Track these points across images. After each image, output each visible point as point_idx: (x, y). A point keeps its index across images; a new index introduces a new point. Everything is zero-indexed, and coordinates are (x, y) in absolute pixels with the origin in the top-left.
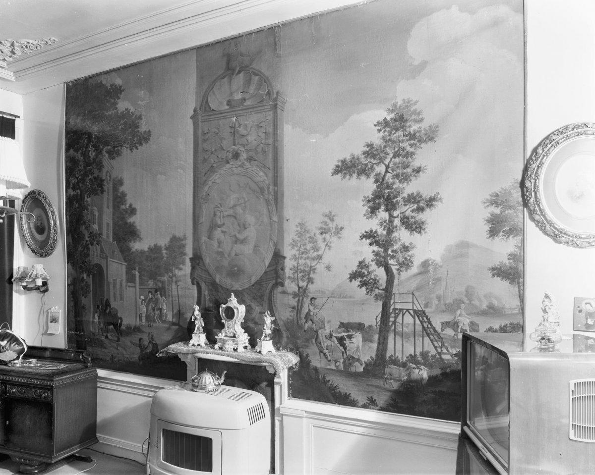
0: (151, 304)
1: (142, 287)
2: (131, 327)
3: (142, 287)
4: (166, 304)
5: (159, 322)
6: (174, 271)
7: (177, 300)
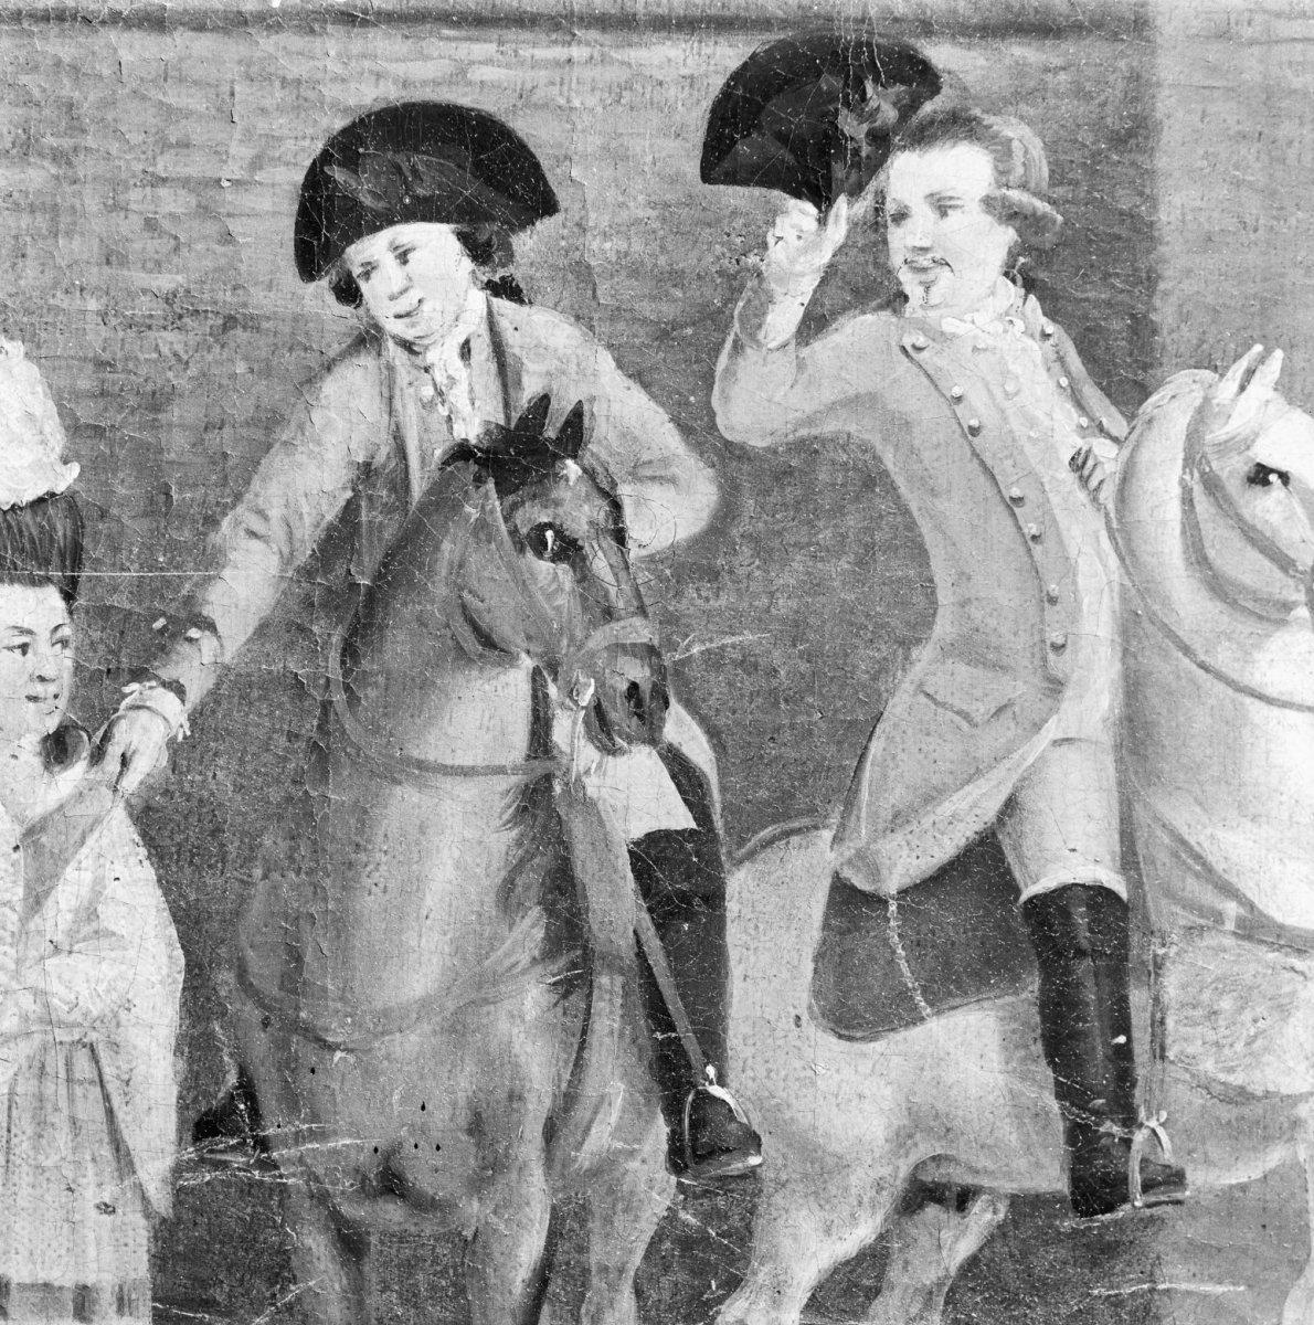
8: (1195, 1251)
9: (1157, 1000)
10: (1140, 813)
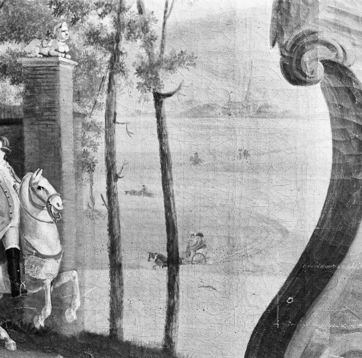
7: (157, 187)
8: (29, 303)
9: (23, 265)
10: (22, 238)
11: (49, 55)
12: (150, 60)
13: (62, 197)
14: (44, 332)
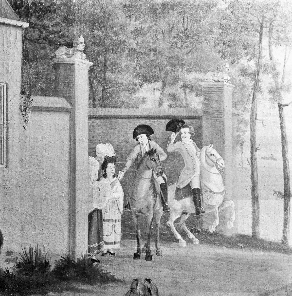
0: (148, 174)
1: (101, 112)
2: (47, 264)
3: (101, 112)
4: (222, 172)
5: (190, 241)
6: (265, 53)
8: (206, 218)
9: (203, 197)
10: (201, 182)
11: (218, 81)
12: (276, 86)
13: (224, 160)
14: (214, 235)
